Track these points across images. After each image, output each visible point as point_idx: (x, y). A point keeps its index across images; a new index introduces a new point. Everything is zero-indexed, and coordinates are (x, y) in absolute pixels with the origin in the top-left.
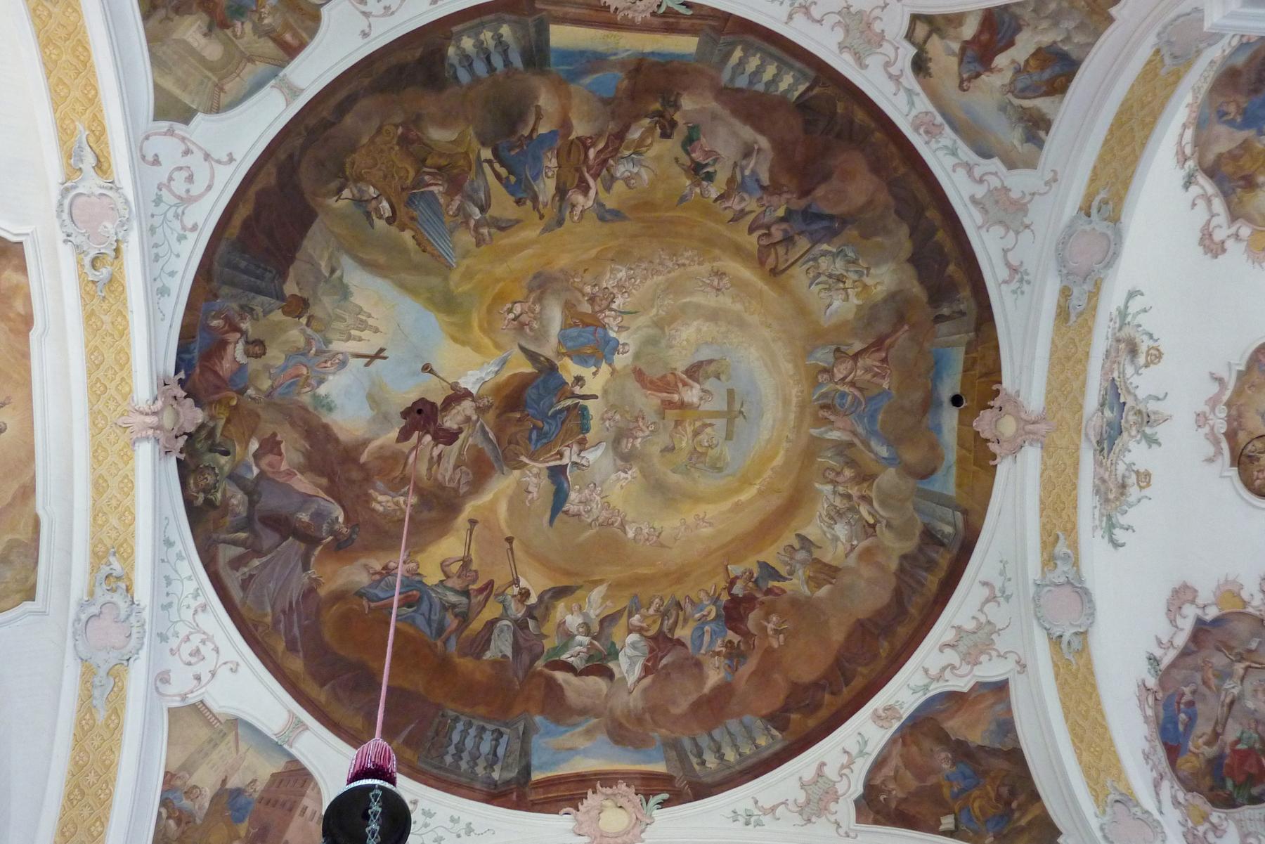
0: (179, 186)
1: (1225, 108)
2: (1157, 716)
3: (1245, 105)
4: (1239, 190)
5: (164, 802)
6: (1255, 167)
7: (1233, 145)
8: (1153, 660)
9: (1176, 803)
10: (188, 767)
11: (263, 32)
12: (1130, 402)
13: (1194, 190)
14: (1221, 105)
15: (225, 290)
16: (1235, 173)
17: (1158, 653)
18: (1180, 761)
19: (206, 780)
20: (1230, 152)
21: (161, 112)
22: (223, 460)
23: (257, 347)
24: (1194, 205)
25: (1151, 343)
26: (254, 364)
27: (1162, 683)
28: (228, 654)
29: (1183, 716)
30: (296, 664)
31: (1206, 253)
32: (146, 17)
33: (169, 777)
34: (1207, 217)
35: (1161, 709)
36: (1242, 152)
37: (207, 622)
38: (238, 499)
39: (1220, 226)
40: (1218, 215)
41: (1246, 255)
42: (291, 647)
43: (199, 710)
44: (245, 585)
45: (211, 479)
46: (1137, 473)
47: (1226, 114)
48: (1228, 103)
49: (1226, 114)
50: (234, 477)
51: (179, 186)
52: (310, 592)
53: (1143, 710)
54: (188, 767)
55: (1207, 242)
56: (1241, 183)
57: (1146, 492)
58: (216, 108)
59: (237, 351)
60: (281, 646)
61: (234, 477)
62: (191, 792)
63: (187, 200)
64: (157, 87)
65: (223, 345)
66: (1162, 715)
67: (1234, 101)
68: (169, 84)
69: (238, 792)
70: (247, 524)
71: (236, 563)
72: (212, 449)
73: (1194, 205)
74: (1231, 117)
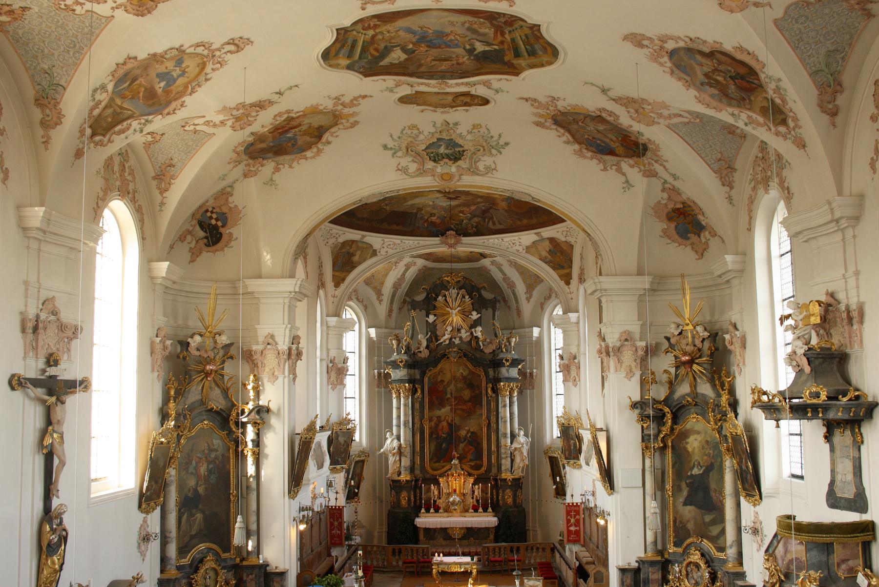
0: (392, 246)
2: (593, 152)
5: (546, 263)
8: (568, 142)
9: (632, 166)
10: (540, 255)
11: (351, 247)
12: (437, 136)
13: (330, 139)
15: (417, 225)
17: (565, 138)
18: (617, 152)
19: (544, 254)
21: (376, 255)
22: (464, 221)
23: (432, 215)
25: (407, 128)
26: (437, 215)
27: (580, 143)
28: (516, 238)
29: (598, 142)
30: (525, 222)
32: (356, 267)
33: (540, 259)
35: (590, 148)
37: (505, 240)
38: (476, 219)
42: (520, 220)
43: (527, 247)
44: (500, 224)
45: (469, 225)
46: (472, 129)
50: (470, 219)
51: (392, 246)
52: (506, 211)
53: (586, 157)
54: (540, 255)
57: (483, 125)
58: (371, 246)
59: (434, 219)
60: (519, 223)
61: (470, 219)
62: (546, 258)
63: (395, 244)
64: (370, 258)
65: (432, 222)
66: (593, 149)
68: (369, 256)
69: (550, 250)
70: (484, 219)
71: (494, 224)
72: (461, 224)
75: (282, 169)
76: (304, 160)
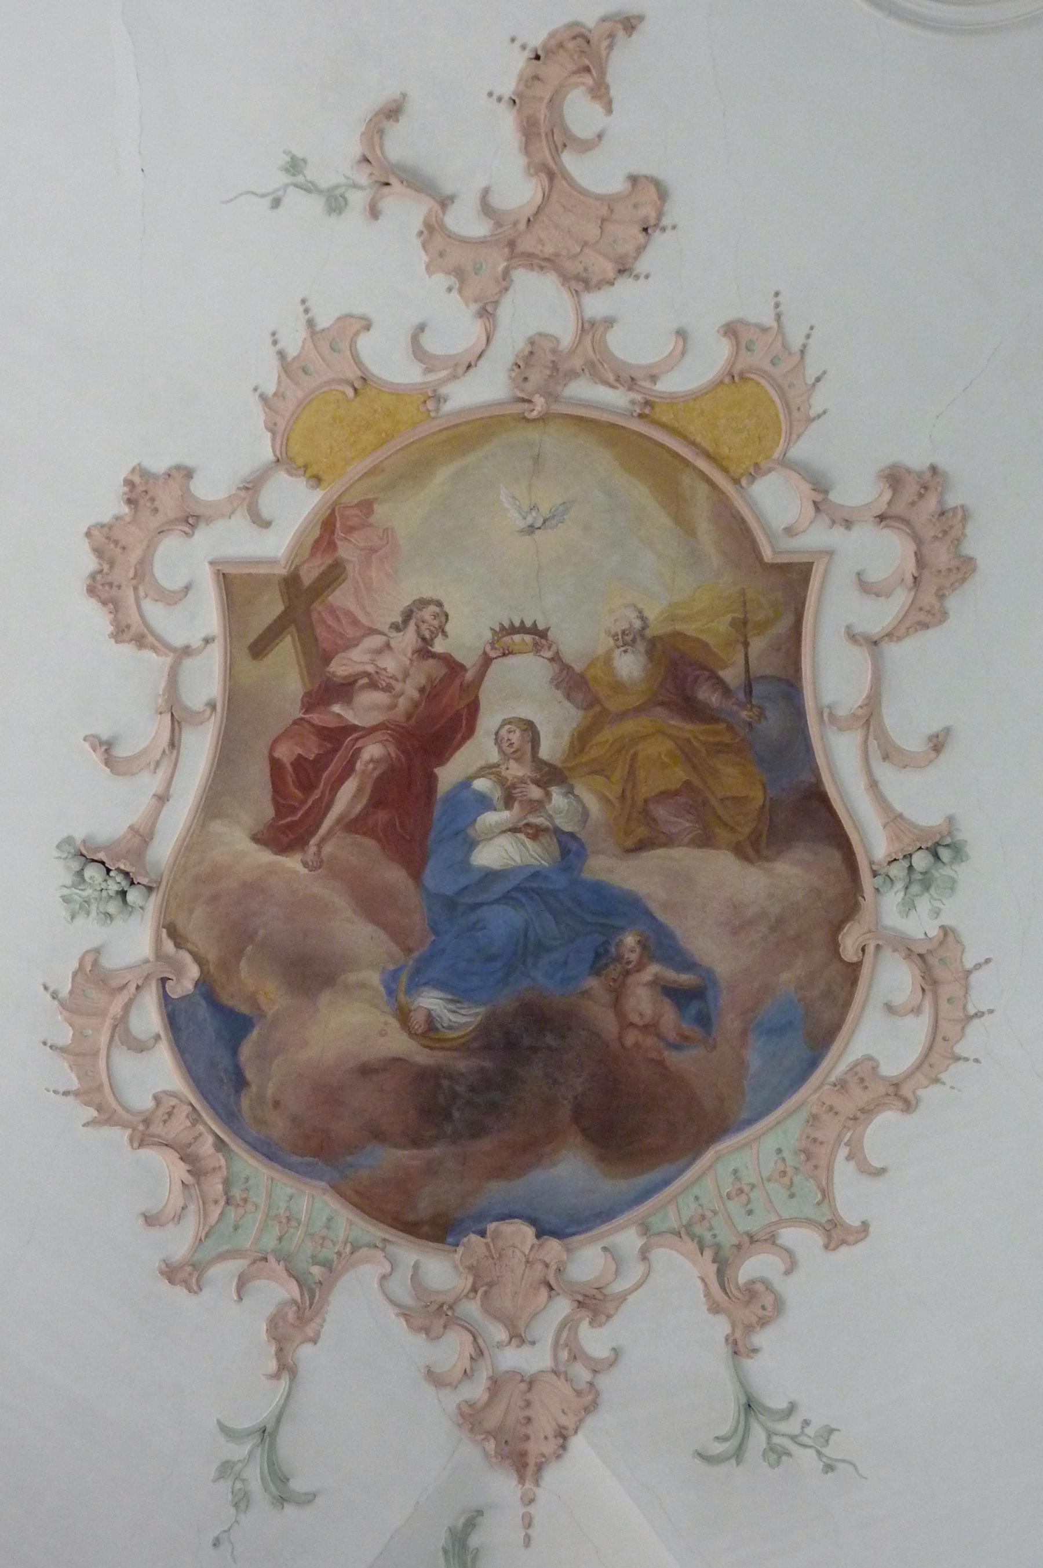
1: (669, 1017)
3: (593, 983)
4: (732, 675)
6: (629, 727)
7: (683, 856)
14: (683, 1042)
16: (720, 749)
20: (705, 841)
24: (938, 744)
31: (965, 514)
34: (895, 652)
36: (660, 812)
39: (865, 587)
40: (853, 637)
41: (818, 403)
47: (679, 996)
48: (651, 1028)
49: (679, 996)
55: (941, 556)
56: (708, 695)
67: (626, 1025)
73: (938, 744)
74: (653, 970)
75: (790, 1288)
76: (888, 1118)
